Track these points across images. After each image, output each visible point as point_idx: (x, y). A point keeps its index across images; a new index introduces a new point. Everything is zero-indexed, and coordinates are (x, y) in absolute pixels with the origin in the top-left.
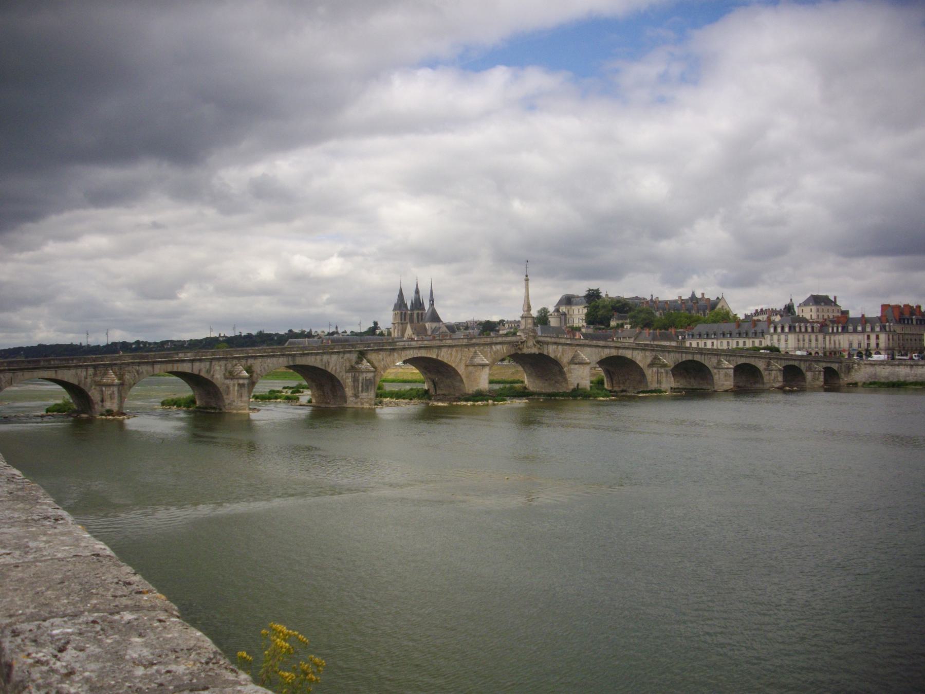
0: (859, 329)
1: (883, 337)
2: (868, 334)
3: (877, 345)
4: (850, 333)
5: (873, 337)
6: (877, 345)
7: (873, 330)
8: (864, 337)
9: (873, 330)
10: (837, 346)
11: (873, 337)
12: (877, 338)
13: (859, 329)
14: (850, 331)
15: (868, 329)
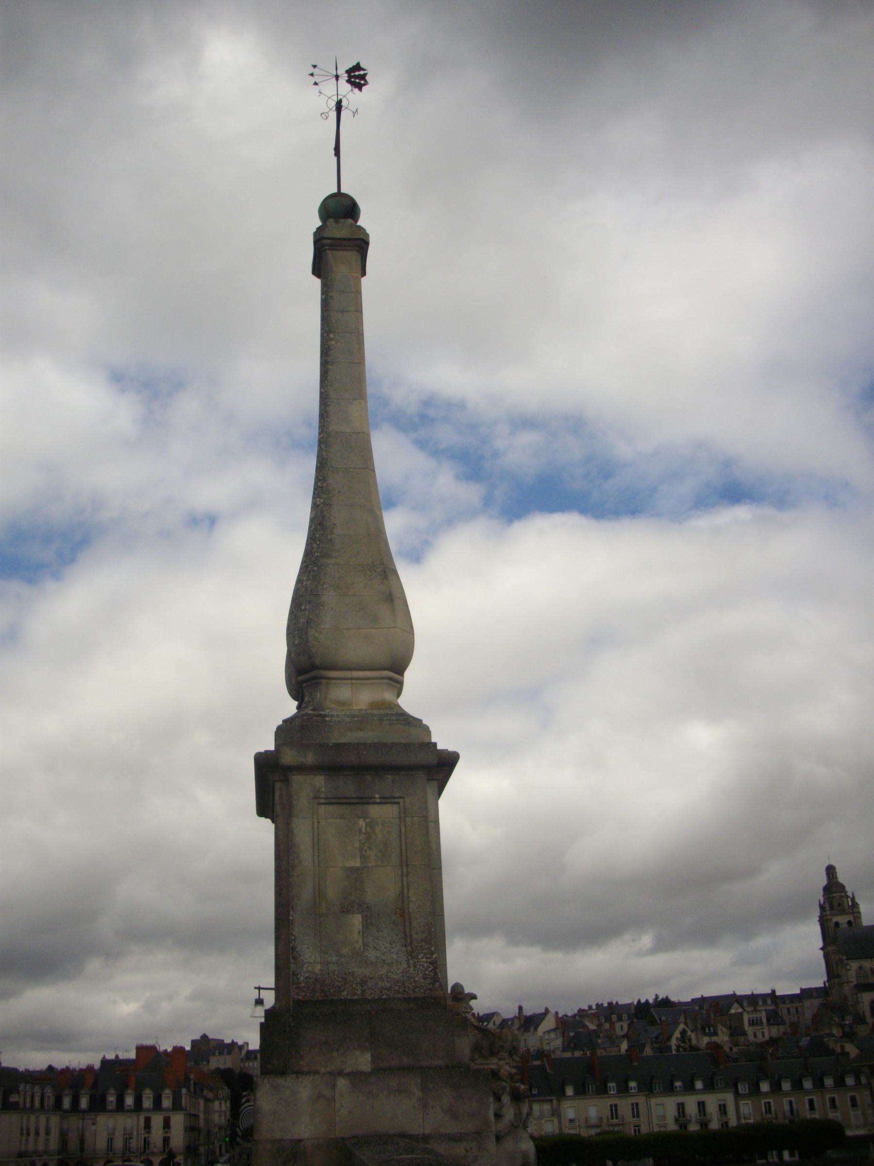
0: (129, 1101)
1: (178, 1121)
2: (148, 1114)
3: (166, 1140)
4: (110, 1111)
5: (157, 1120)
6: (166, 1140)
7: (157, 1105)
8: (138, 1121)
9: (157, 1105)
10: (73, 1144)
11: (157, 1120)
12: (167, 1124)
13: (129, 1101)
14: (110, 1107)
15: (147, 1103)
